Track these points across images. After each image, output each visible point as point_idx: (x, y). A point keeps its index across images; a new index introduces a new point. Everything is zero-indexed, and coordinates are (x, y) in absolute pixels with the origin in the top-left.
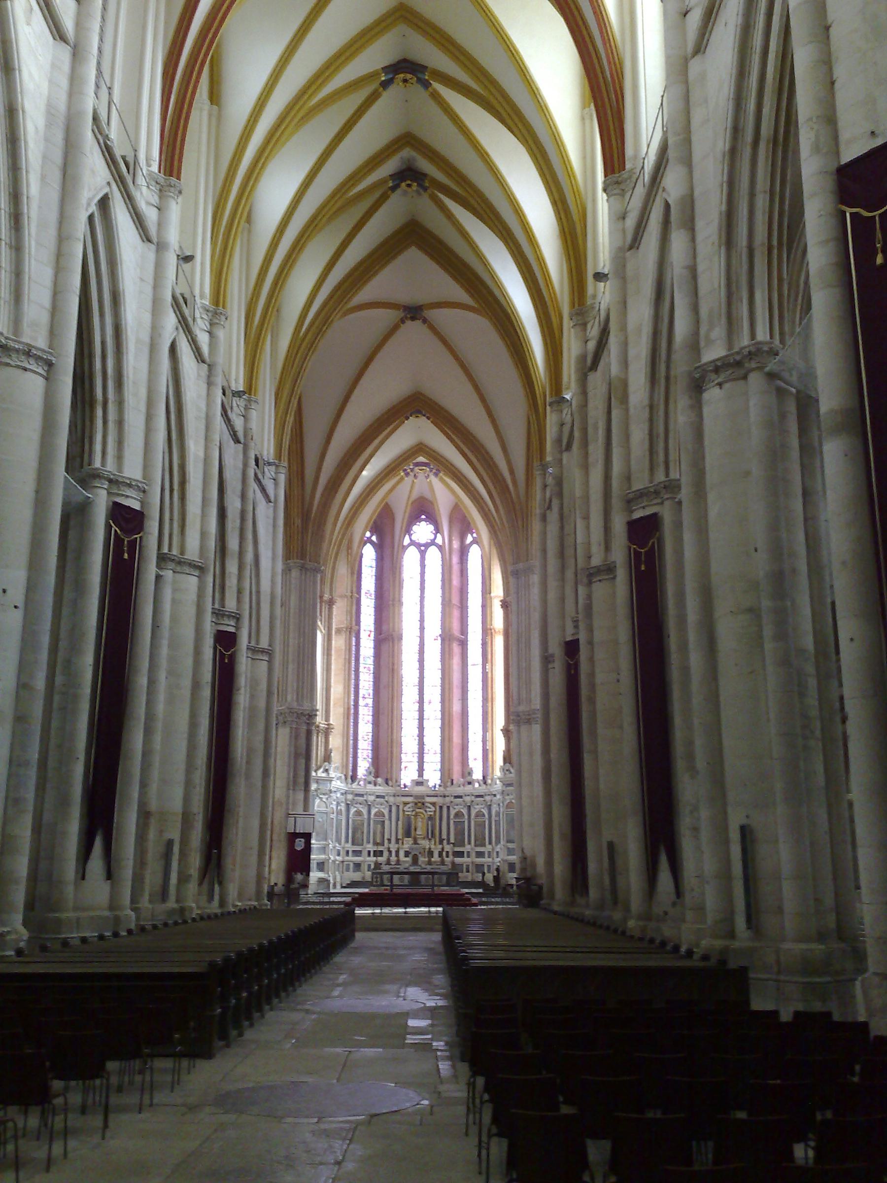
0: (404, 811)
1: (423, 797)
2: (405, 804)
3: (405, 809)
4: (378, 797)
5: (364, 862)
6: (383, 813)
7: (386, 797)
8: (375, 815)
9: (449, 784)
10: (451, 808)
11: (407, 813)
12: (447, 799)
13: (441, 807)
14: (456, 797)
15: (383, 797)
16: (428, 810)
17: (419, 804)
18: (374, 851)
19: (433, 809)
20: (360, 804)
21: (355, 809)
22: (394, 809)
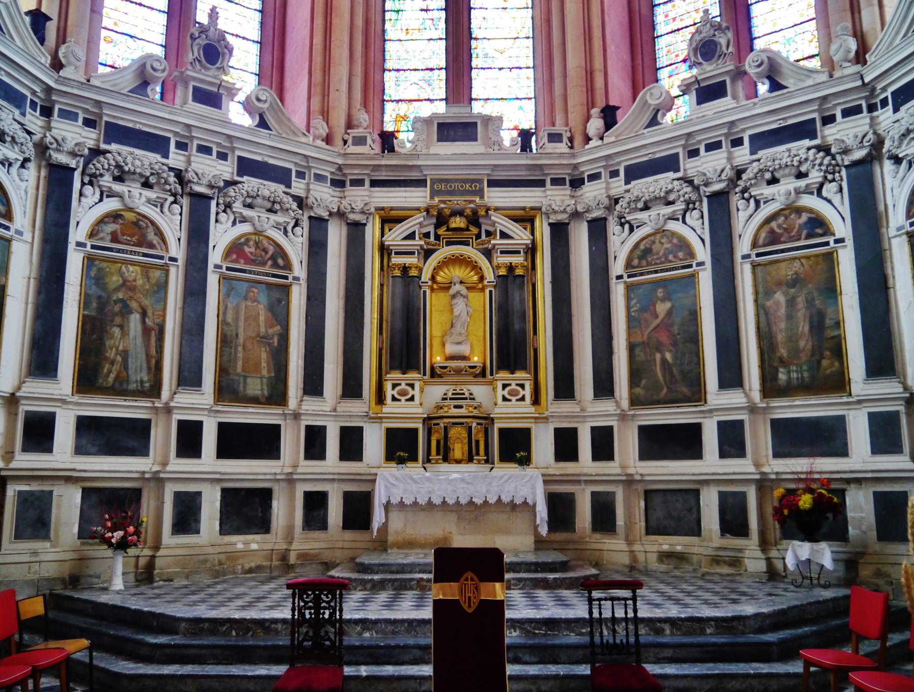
0: (384, 250)
1: (473, 187)
2: (390, 219)
3: (395, 236)
4: (246, 167)
5: (158, 481)
6: (280, 252)
7: (298, 187)
8: (235, 249)
9: (595, 124)
10: (613, 227)
11: (396, 260)
12: (592, 192)
13: (560, 232)
14: (634, 173)
15: (282, 176)
16: (497, 241)
17: (458, 222)
18: (224, 429)
19: (520, 236)
20: (146, 185)
21: (111, 205)
22: (336, 237)
